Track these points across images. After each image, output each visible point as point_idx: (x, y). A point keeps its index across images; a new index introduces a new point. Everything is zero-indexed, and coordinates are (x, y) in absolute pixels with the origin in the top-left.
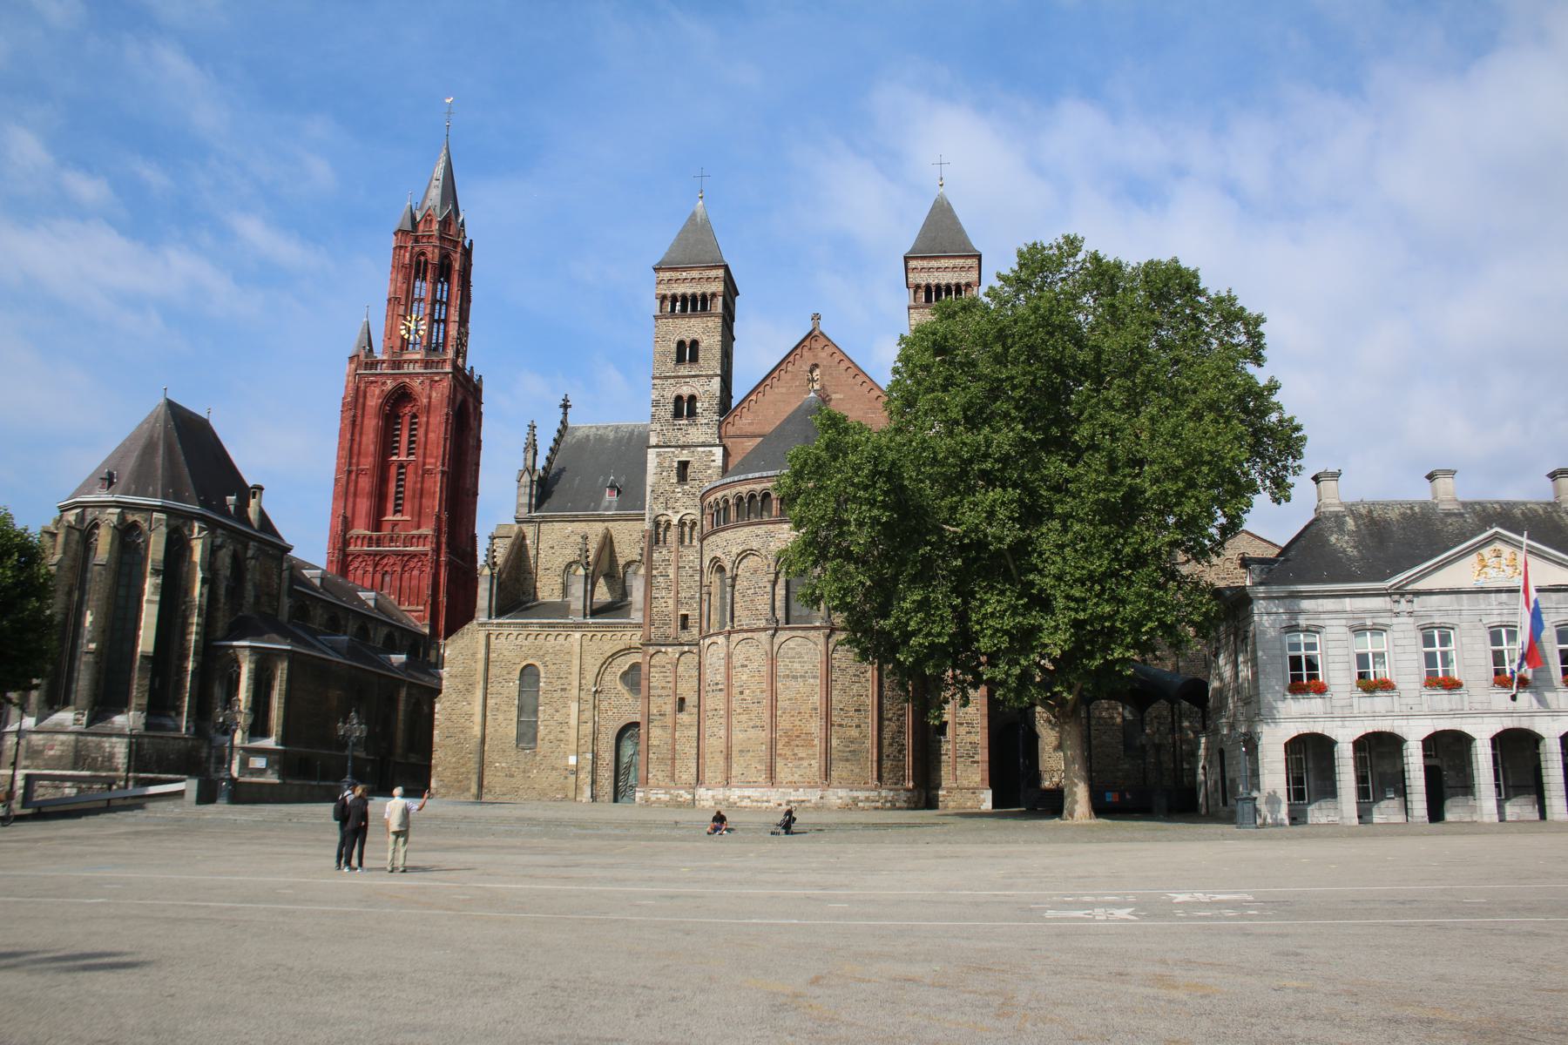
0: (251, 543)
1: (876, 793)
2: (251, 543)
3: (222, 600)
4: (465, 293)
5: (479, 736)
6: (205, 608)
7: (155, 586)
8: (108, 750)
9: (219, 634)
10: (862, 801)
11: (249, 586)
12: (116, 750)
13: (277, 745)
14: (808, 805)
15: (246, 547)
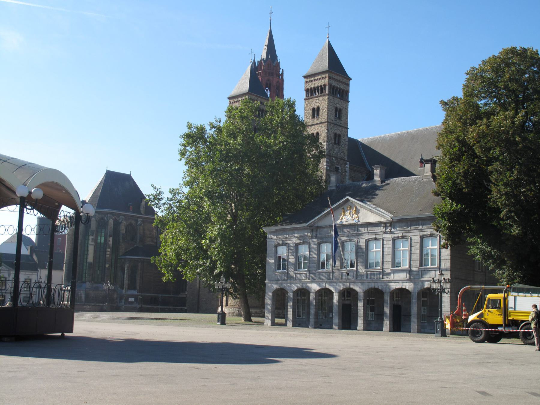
0: (139, 219)
1: (260, 310)
2: (139, 219)
3: (121, 242)
4: (281, 94)
5: (198, 288)
6: (111, 245)
7: (93, 239)
8: (80, 295)
9: (120, 254)
10: (253, 313)
11: (138, 235)
12: (82, 295)
13: (138, 293)
14: (234, 314)
15: (137, 221)
